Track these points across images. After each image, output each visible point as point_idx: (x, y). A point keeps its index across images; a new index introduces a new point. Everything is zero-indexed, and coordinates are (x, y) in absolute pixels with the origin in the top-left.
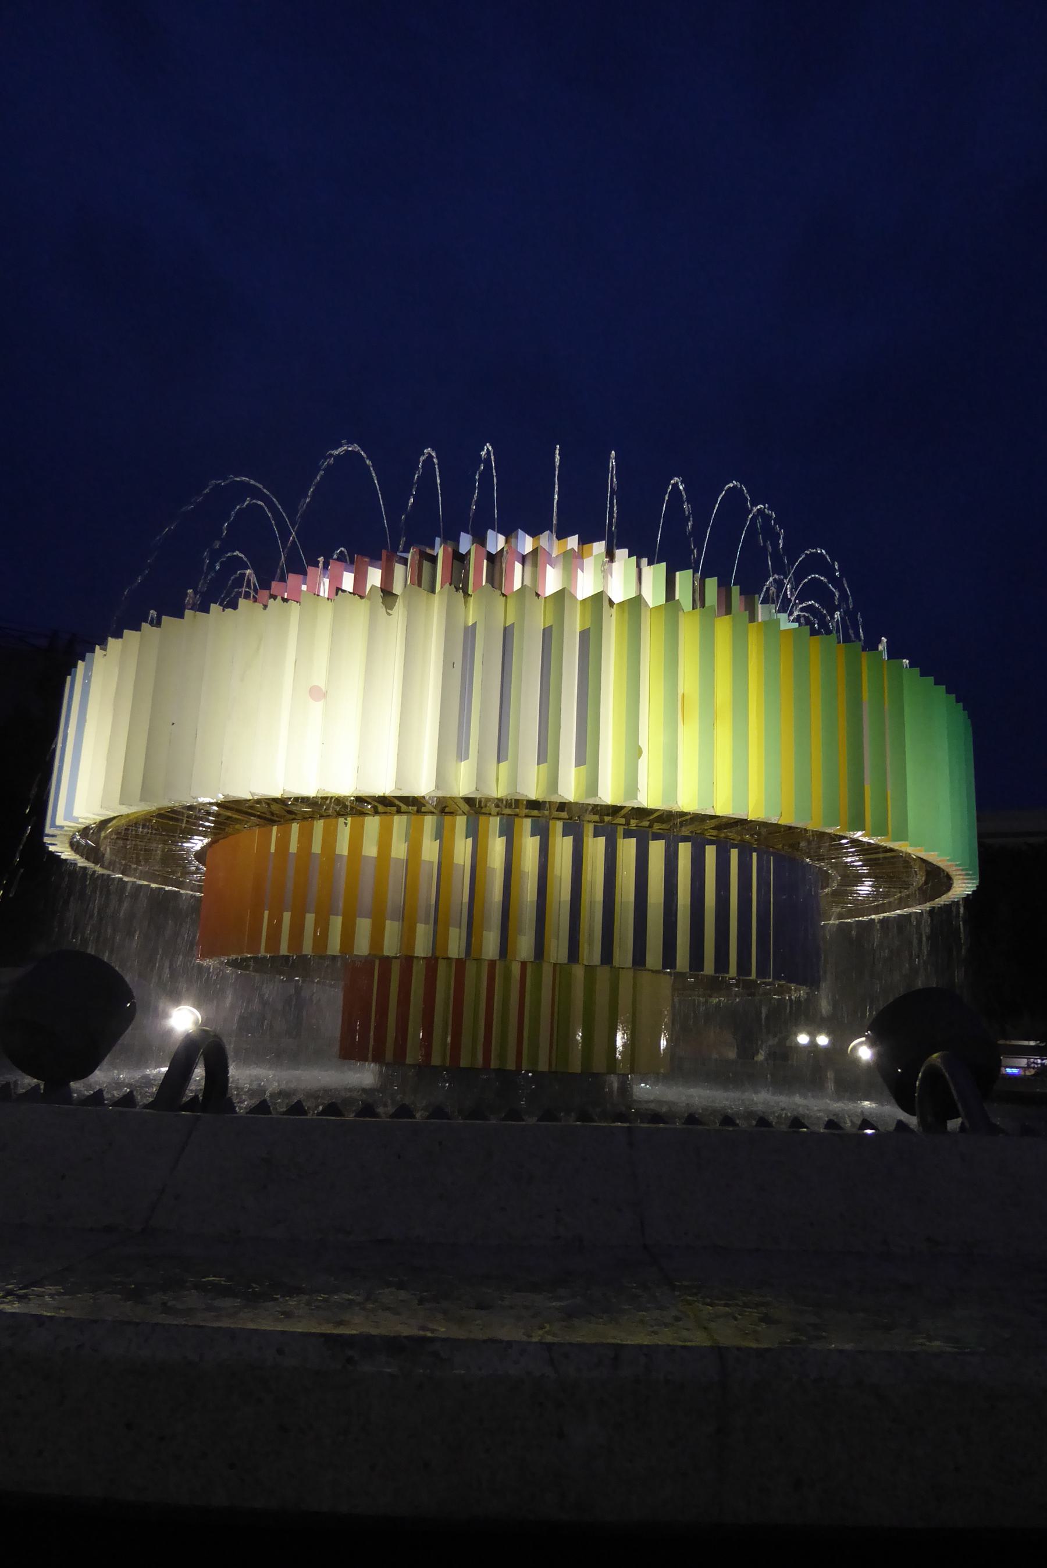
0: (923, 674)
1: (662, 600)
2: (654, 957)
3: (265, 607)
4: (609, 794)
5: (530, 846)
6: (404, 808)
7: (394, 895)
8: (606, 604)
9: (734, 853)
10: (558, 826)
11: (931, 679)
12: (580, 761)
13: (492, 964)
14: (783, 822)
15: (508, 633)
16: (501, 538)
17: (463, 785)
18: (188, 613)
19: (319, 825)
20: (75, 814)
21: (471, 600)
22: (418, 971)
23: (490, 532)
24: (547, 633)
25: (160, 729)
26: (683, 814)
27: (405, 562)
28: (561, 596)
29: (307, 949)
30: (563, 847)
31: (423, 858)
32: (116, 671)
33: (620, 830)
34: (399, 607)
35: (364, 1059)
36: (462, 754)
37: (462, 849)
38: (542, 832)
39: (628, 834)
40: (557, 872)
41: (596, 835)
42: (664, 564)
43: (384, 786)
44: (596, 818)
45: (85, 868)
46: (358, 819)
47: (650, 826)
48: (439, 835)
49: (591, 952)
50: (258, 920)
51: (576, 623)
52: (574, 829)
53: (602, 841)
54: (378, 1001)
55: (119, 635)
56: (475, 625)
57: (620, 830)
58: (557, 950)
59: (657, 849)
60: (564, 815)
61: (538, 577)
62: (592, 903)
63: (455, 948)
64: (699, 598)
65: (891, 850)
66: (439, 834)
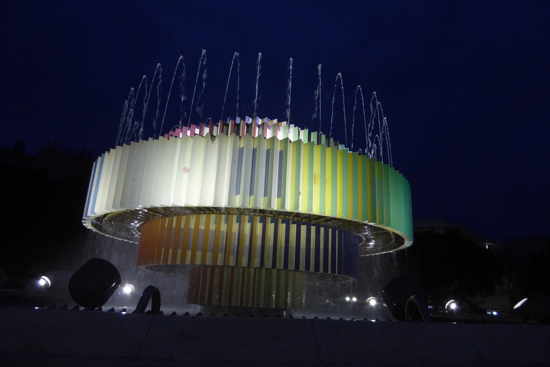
3: (169, 139)
4: (289, 208)
5: (259, 227)
6: (215, 211)
7: (210, 243)
8: (289, 142)
12: (279, 196)
13: (244, 268)
14: (348, 219)
15: (254, 151)
16: (251, 119)
17: (237, 203)
18: (141, 140)
20: (95, 211)
21: (242, 139)
22: (217, 272)
23: (247, 117)
24: (268, 151)
25: (128, 183)
26: (314, 215)
27: (217, 126)
28: (274, 139)
29: (178, 262)
30: (271, 227)
34: (216, 141)
35: (196, 303)
36: (238, 193)
37: (235, 227)
39: (293, 223)
40: (269, 236)
43: (209, 203)
44: (283, 217)
46: (198, 215)
47: (302, 220)
49: (280, 264)
50: (160, 252)
51: (278, 148)
53: (284, 225)
54: (205, 280)
56: (243, 148)
58: (268, 264)
59: (304, 228)
60: (272, 215)
62: (281, 247)
63: (232, 262)
66: (227, 221)
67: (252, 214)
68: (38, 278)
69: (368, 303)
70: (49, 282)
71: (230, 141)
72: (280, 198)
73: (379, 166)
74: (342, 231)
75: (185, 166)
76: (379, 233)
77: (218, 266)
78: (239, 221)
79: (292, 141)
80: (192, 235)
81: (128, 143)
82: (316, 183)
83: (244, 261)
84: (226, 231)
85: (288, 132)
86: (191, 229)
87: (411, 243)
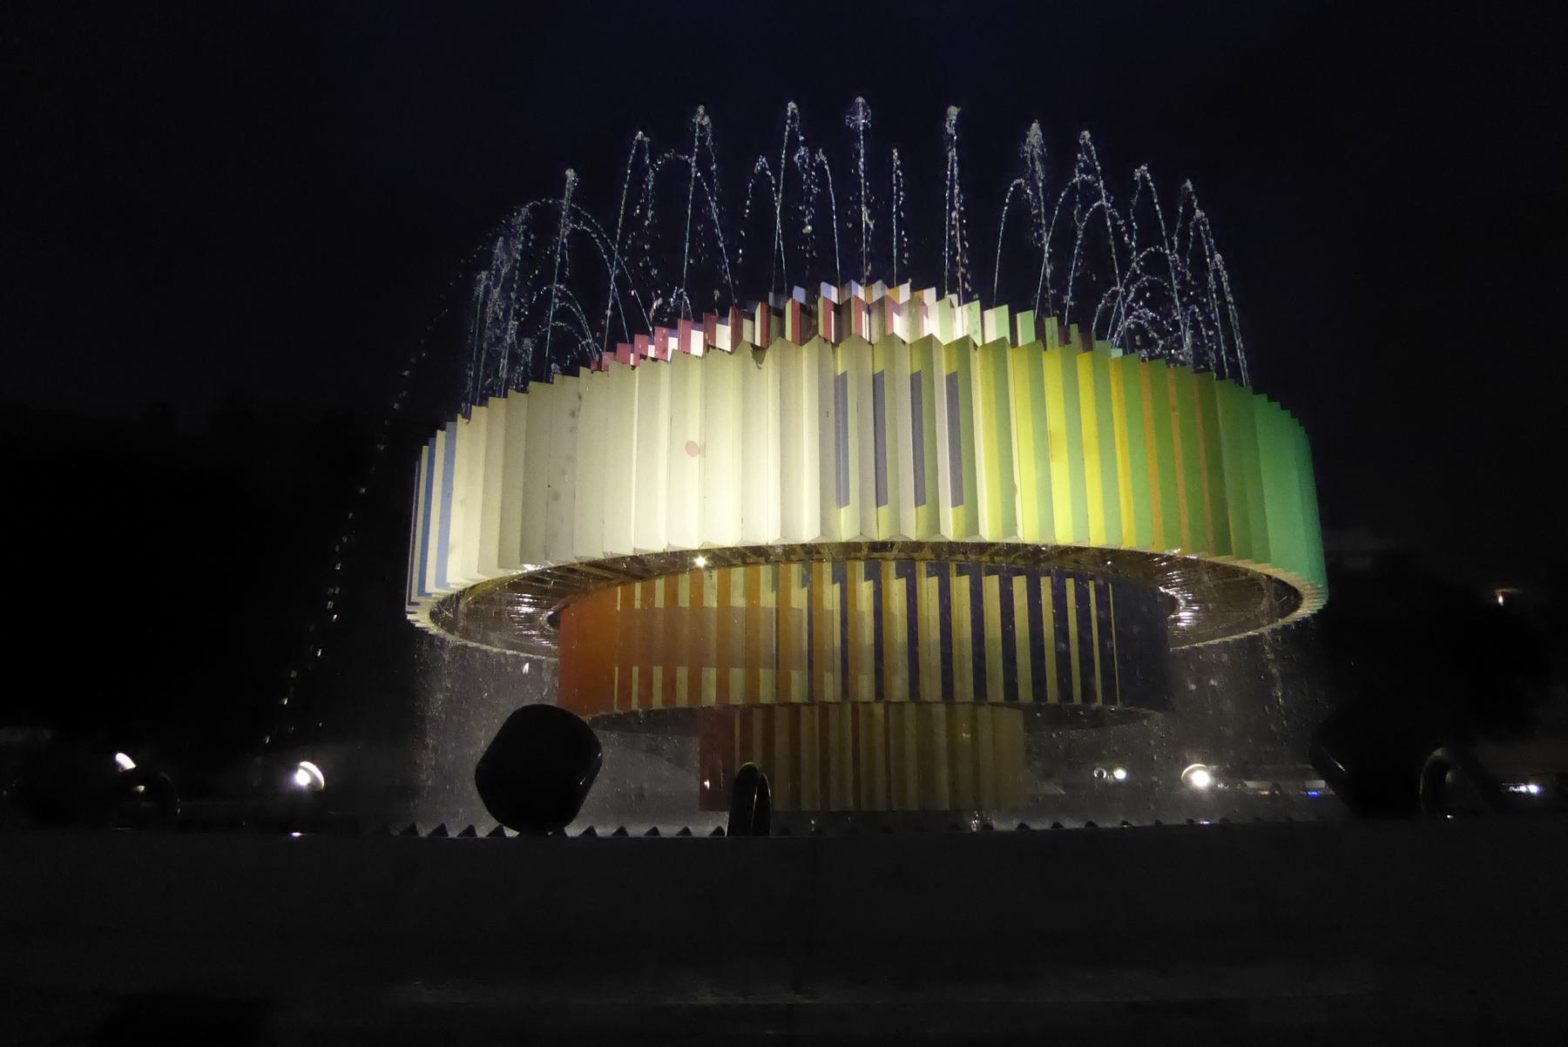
1: (1032, 338)
2: (996, 691)
4: (988, 532)
5: (897, 589)
9: (1070, 583)
11: (1277, 404)
12: (957, 501)
15: (878, 381)
16: (834, 290)
17: (846, 529)
18: (557, 378)
19: (660, 584)
20: (449, 580)
21: (839, 350)
23: (824, 285)
24: (916, 379)
25: (535, 493)
30: (929, 587)
33: (953, 567)
36: (843, 500)
37: (831, 595)
38: (874, 574)
39: (991, 572)
41: (929, 575)
42: (1006, 307)
43: (768, 534)
44: (960, 557)
49: (965, 687)
51: (943, 368)
52: (907, 571)
55: (483, 402)
56: (844, 374)
57: (953, 567)
59: (1019, 584)
61: (885, 323)
63: (831, 690)
64: (1065, 339)
65: (1246, 572)
66: (806, 581)
67: (876, 555)
69: (1188, 781)
71: (806, 357)
73: (1223, 392)
74: (1118, 583)
75: (691, 438)
79: (979, 344)
80: (713, 628)
82: (1061, 460)
83: (865, 687)
84: (837, 607)
85: (949, 321)
86: (708, 608)
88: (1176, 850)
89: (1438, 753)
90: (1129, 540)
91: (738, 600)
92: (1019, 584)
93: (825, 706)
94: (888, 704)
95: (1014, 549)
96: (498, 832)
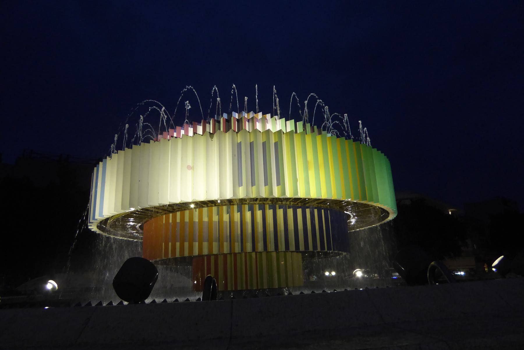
0: (378, 150)
2: (292, 247)
4: (289, 194)
5: (259, 214)
9: (316, 211)
10: (257, 206)
11: (380, 152)
12: (278, 184)
15: (251, 144)
16: (237, 114)
17: (241, 194)
19: (178, 214)
20: (103, 214)
21: (239, 134)
22: (221, 259)
23: (233, 113)
24: (264, 144)
25: (134, 184)
26: (312, 199)
30: (270, 213)
31: (214, 220)
32: (116, 165)
36: (240, 184)
37: (237, 216)
39: (289, 208)
42: (293, 120)
43: (215, 196)
44: (280, 203)
45: (99, 234)
47: (297, 204)
48: (218, 214)
51: (273, 140)
52: (262, 208)
53: (282, 210)
56: (241, 142)
57: (277, 206)
59: (299, 211)
61: (254, 126)
62: (280, 231)
64: (313, 131)
68: (46, 283)
69: (355, 275)
70: (56, 285)
71: (228, 137)
72: (280, 186)
74: (331, 211)
76: (363, 210)
77: (214, 255)
78: (240, 210)
79: (285, 132)
81: (129, 147)
82: (312, 170)
83: (249, 247)
85: (276, 125)
87: (395, 216)
88: (353, 298)
89: (433, 263)
90: (334, 196)
91: (205, 219)
92: (299, 211)
93: (235, 254)
94: (256, 253)
95: (296, 200)
96: (121, 303)
